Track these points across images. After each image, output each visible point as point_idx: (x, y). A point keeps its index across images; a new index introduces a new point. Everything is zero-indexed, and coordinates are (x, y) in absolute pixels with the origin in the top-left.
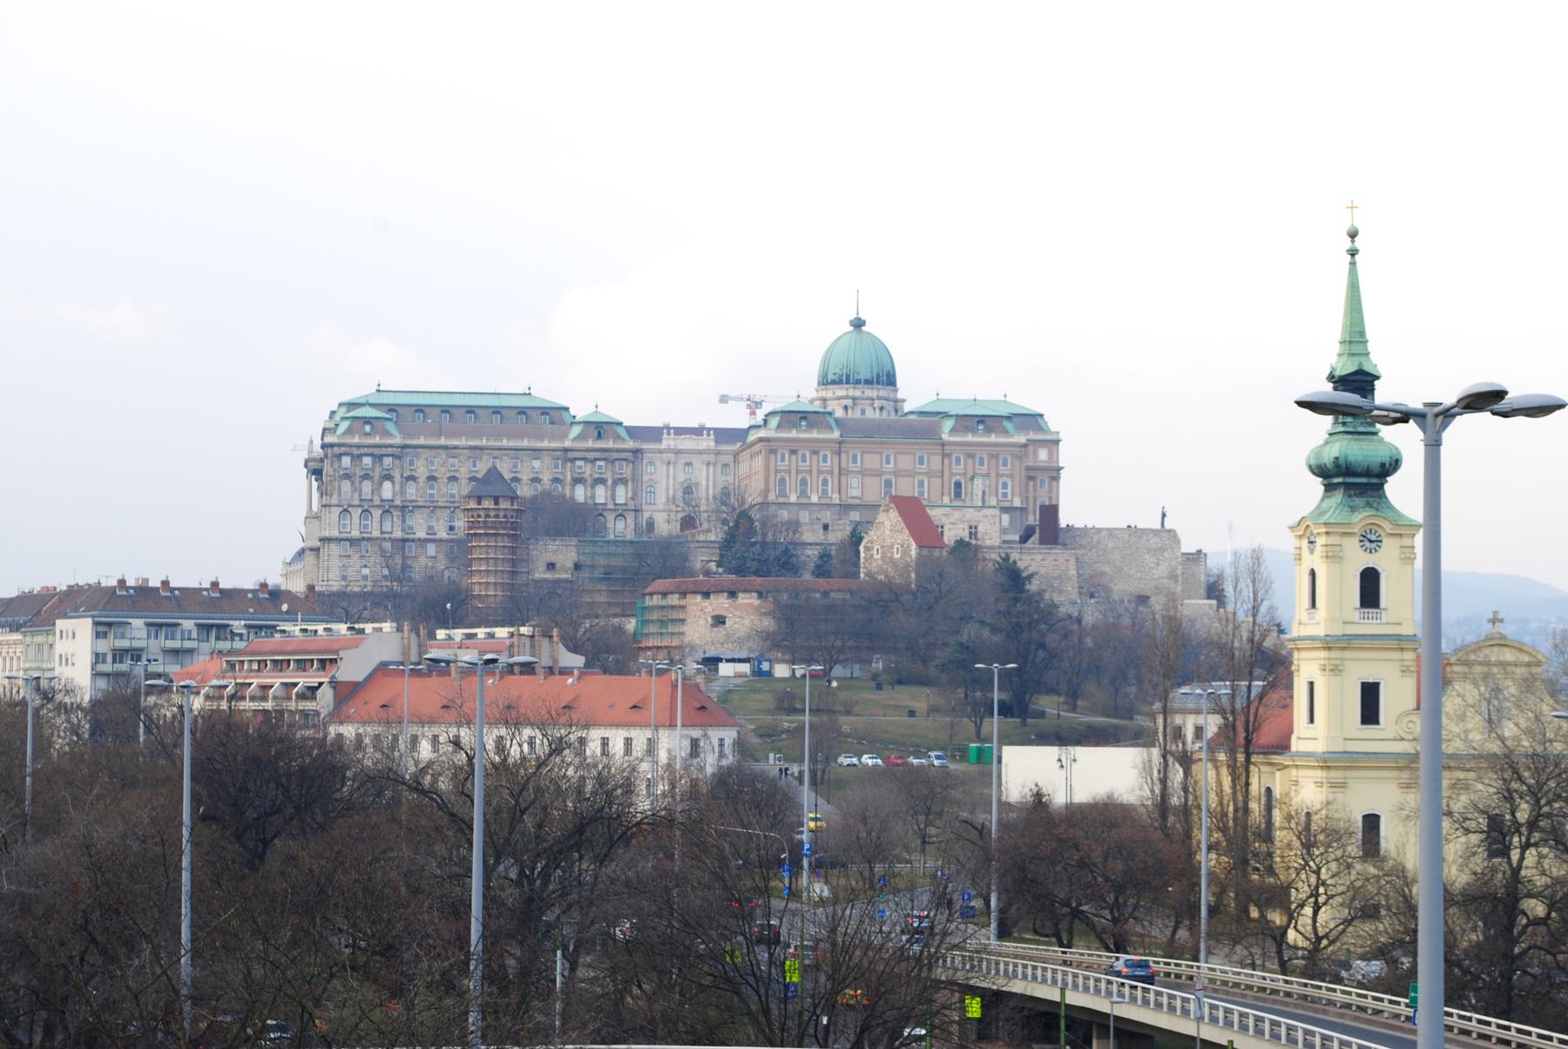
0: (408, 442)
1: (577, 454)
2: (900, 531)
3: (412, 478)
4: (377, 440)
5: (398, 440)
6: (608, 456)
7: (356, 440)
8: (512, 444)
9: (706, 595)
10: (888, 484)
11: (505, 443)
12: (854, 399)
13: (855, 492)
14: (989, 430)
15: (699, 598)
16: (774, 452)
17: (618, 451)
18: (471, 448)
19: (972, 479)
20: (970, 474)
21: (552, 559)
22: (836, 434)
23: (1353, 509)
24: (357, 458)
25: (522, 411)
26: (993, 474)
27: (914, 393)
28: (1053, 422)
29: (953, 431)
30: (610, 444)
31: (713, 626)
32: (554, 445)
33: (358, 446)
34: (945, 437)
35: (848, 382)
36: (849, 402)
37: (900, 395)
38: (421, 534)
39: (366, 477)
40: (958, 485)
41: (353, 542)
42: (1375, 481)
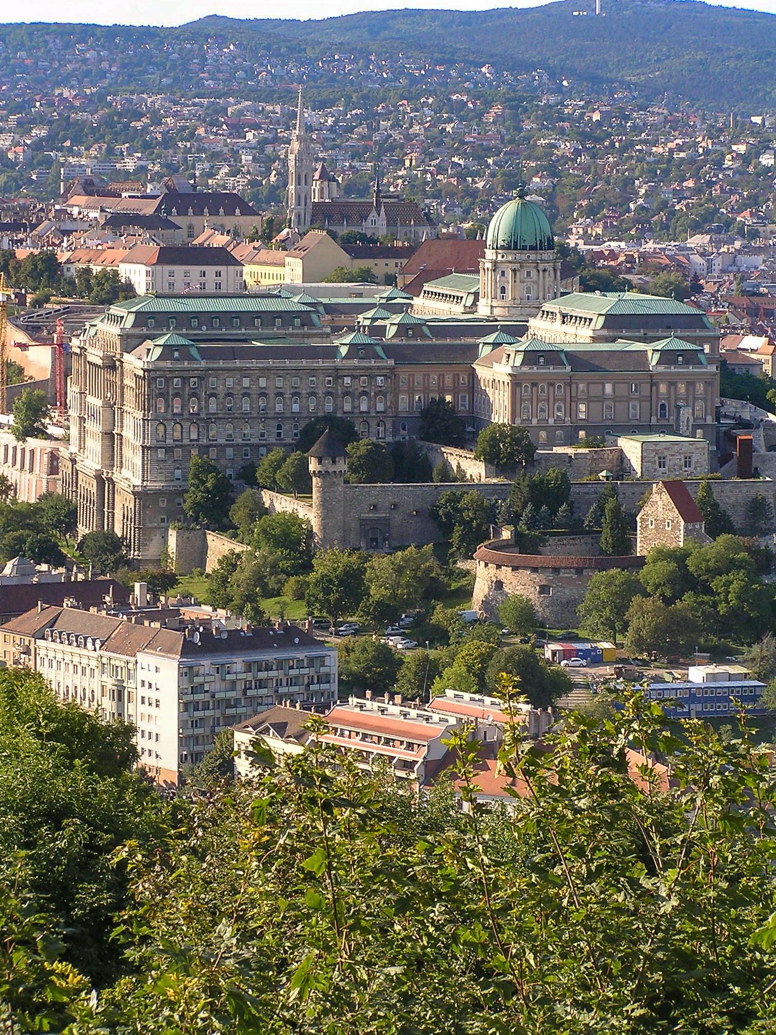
1: (346, 372)
3: (214, 395)
5: (203, 364)
9: (535, 570)
14: (687, 363)
18: (261, 369)
21: (372, 500)
26: (691, 398)
31: (540, 593)
32: (327, 364)
35: (515, 248)
36: (517, 266)
39: (177, 395)
40: (663, 406)
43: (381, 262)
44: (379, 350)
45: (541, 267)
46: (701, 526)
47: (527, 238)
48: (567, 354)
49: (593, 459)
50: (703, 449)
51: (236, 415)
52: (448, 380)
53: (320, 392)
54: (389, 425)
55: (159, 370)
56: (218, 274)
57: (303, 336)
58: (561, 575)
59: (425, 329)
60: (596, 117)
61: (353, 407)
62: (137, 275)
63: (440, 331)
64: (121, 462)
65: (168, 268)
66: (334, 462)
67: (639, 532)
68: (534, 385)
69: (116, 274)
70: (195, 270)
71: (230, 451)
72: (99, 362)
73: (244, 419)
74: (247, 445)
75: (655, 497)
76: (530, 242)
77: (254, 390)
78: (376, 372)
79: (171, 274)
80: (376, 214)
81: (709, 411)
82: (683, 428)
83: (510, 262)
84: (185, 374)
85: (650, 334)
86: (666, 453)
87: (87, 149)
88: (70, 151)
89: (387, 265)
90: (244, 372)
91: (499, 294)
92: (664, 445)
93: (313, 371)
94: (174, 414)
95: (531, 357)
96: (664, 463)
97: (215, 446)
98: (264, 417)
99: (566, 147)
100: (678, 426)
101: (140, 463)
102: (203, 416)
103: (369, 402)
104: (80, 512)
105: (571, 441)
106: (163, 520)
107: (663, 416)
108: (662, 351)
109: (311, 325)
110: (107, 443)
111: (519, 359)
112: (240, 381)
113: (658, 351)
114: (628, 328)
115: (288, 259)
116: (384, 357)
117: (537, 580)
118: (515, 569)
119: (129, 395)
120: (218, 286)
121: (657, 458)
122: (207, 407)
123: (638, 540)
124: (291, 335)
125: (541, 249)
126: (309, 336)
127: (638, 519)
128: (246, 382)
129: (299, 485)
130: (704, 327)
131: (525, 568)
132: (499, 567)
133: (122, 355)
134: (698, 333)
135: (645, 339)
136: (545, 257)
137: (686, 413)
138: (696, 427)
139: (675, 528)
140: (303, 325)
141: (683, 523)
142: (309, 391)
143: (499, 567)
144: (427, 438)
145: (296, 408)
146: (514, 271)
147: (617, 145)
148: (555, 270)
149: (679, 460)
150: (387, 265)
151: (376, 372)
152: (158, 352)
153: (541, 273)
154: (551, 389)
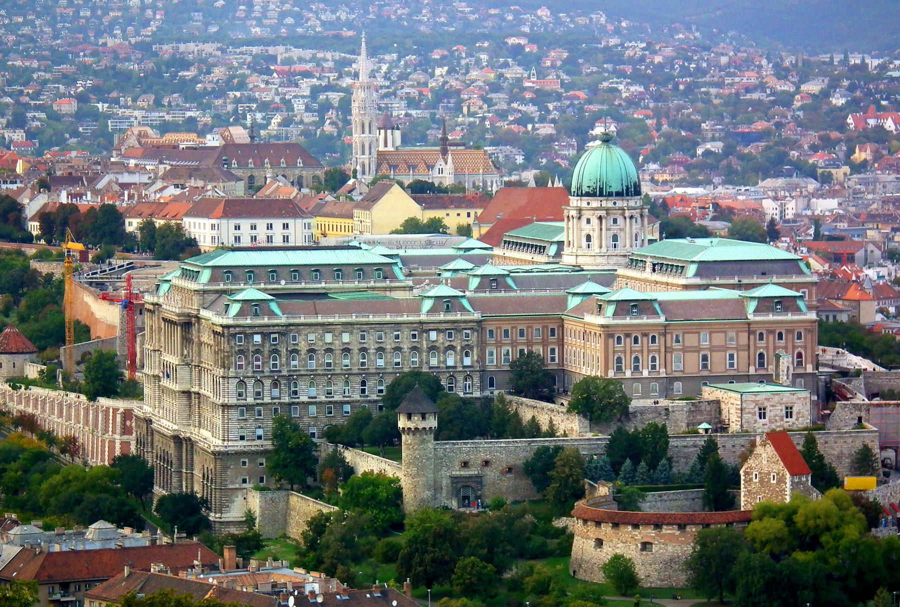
1: (432, 326)
2: (776, 463)
4: (266, 321)
5: (283, 320)
7: (249, 321)
8: (377, 319)
9: (636, 526)
10: (705, 358)
11: (371, 319)
12: (607, 210)
14: (786, 310)
15: (630, 528)
16: (610, 336)
18: (343, 324)
21: (464, 457)
30: (459, 317)
31: (642, 550)
32: (412, 318)
33: (251, 327)
34: (751, 317)
35: (601, 195)
36: (603, 213)
38: (303, 398)
39: (257, 351)
40: (761, 356)
41: (250, 407)
43: (453, 212)
44: (465, 302)
45: (627, 214)
46: (807, 479)
47: (614, 185)
48: (661, 304)
49: (690, 411)
50: (805, 398)
51: (319, 372)
53: (406, 347)
54: (476, 380)
55: (238, 326)
56: (286, 226)
57: (385, 289)
58: (664, 531)
59: (509, 281)
60: (658, 59)
61: (439, 362)
62: (200, 229)
63: (524, 283)
64: (200, 422)
65: (233, 222)
66: (424, 418)
67: (742, 486)
68: (628, 335)
69: (179, 227)
70: (262, 224)
71: (313, 409)
72: (175, 318)
73: (327, 375)
74: (330, 402)
75: (759, 450)
76: (616, 188)
77: (337, 346)
78: (463, 325)
79: (237, 228)
80: (443, 163)
81: (809, 359)
82: (783, 378)
84: (265, 330)
85: (745, 281)
86: (766, 404)
87: (135, 100)
88: (116, 101)
89: (458, 215)
91: (584, 243)
92: (764, 396)
95: (625, 307)
96: (764, 413)
97: (298, 403)
98: (348, 375)
99: (627, 90)
100: (778, 375)
101: (219, 422)
102: (285, 373)
103: (455, 357)
104: (156, 475)
105: (667, 392)
106: (244, 481)
107: (761, 365)
108: (762, 300)
109: (394, 278)
110: (184, 401)
111: (611, 310)
112: (323, 336)
113: (755, 298)
114: (722, 275)
115: (355, 211)
116: (470, 309)
117: (639, 537)
118: (616, 525)
119: (206, 353)
120: (286, 239)
121: (757, 409)
122: (288, 364)
123: (742, 494)
124: (373, 289)
125: (627, 195)
126: (391, 289)
127: (742, 473)
128: (329, 338)
129: (387, 442)
130: (801, 273)
131: (627, 524)
132: (598, 524)
133: (198, 310)
134: (795, 279)
135: (739, 286)
136: (632, 203)
137: (786, 362)
138: (796, 376)
139: (781, 480)
140: (385, 278)
141: (788, 476)
142: (393, 346)
143: (598, 524)
144: (518, 393)
145: (381, 362)
146: (600, 218)
147: (681, 87)
148: (642, 216)
149: (780, 411)
150: (458, 215)
151: (463, 325)
152: (235, 308)
153: (628, 220)
154: (645, 339)
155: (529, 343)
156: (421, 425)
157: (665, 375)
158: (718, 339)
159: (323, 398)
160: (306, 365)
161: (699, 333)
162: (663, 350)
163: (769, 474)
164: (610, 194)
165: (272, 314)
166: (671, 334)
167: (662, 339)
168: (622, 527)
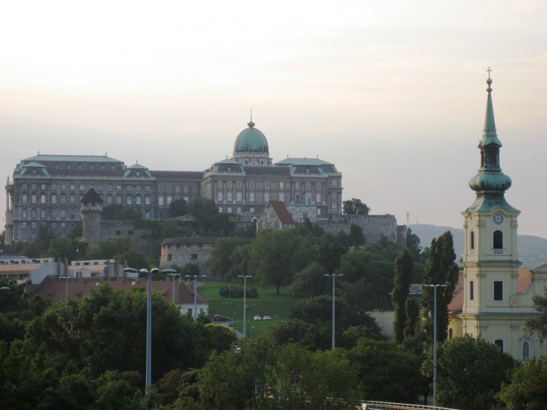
0: (53, 178)
4: (39, 177)
5: (48, 177)
6: (142, 184)
7: (30, 177)
9: (189, 245)
11: (96, 178)
12: (250, 158)
13: (252, 200)
14: (311, 172)
15: (185, 247)
17: (146, 181)
19: (304, 193)
20: (303, 191)
22: (244, 174)
23: (490, 205)
24: (29, 185)
25: (103, 164)
27: (277, 155)
28: (339, 168)
29: (296, 172)
30: (143, 178)
33: (31, 180)
34: (292, 175)
35: (247, 151)
36: (248, 160)
37: (270, 157)
39: (34, 193)
41: (29, 223)
42: (499, 192)
45: (260, 160)
52: (186, 190)
53: (114, 194)
54: (152, 212)
58: (204, 248)
74: (72, 222)
75: (266, 210)
76: (254, 147)
83: (244, 158)
90: (72, 182)
93: (110, 182)
94: (32, 204)
118: (178, 246)
125: (261, 151)
127: (257, 224)
128: (73, 187)
131: (183, 244)
141: (280, 223)
142: (108, 193)
154: (234, 184)
155: (182, 194)
156: (93, 208)
157: (244, 204)
158: (274, 186)
159: (69, 219)
160: (60, 201)
161: (264, 182)
162: (244, 190)
163: (271, 223)
164: (252, 151)
165: (42, 174)
166: (249, 182)
167: (244, 185)
168: (181, 246)
